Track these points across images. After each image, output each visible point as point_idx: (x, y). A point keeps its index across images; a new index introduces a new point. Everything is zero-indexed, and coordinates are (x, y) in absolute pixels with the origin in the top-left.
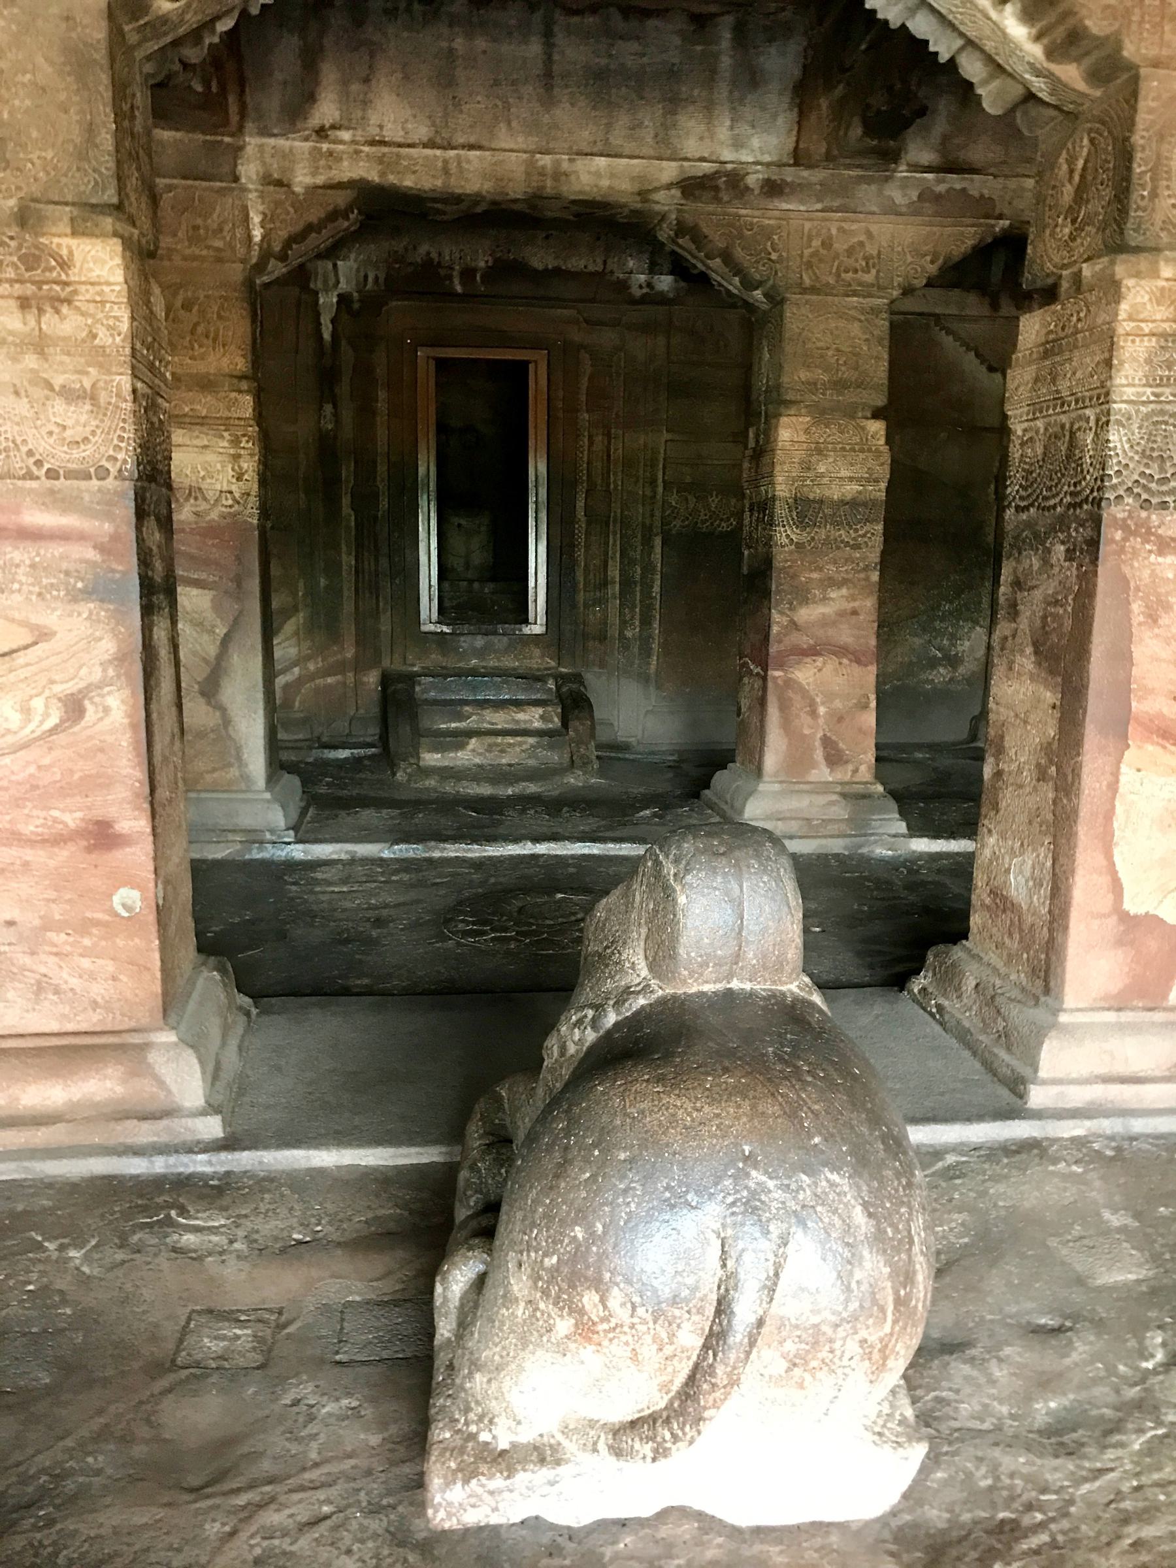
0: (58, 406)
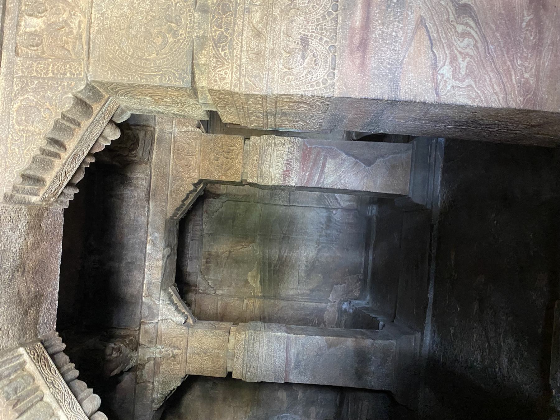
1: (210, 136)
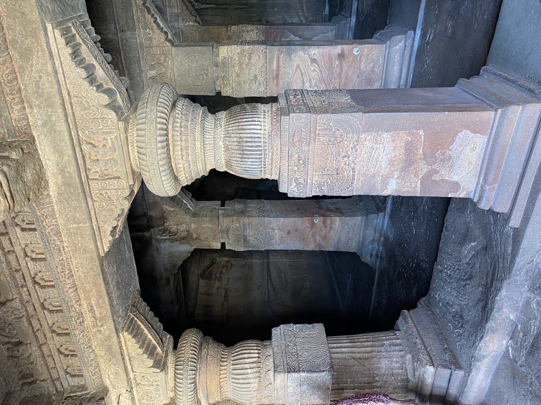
0: (252, 61)
1: (205, 28)
